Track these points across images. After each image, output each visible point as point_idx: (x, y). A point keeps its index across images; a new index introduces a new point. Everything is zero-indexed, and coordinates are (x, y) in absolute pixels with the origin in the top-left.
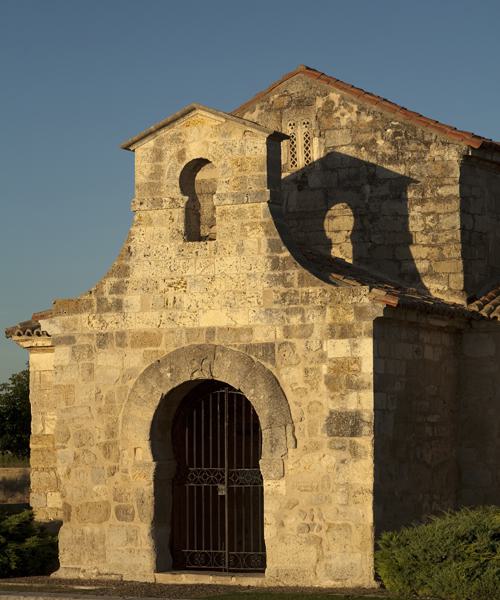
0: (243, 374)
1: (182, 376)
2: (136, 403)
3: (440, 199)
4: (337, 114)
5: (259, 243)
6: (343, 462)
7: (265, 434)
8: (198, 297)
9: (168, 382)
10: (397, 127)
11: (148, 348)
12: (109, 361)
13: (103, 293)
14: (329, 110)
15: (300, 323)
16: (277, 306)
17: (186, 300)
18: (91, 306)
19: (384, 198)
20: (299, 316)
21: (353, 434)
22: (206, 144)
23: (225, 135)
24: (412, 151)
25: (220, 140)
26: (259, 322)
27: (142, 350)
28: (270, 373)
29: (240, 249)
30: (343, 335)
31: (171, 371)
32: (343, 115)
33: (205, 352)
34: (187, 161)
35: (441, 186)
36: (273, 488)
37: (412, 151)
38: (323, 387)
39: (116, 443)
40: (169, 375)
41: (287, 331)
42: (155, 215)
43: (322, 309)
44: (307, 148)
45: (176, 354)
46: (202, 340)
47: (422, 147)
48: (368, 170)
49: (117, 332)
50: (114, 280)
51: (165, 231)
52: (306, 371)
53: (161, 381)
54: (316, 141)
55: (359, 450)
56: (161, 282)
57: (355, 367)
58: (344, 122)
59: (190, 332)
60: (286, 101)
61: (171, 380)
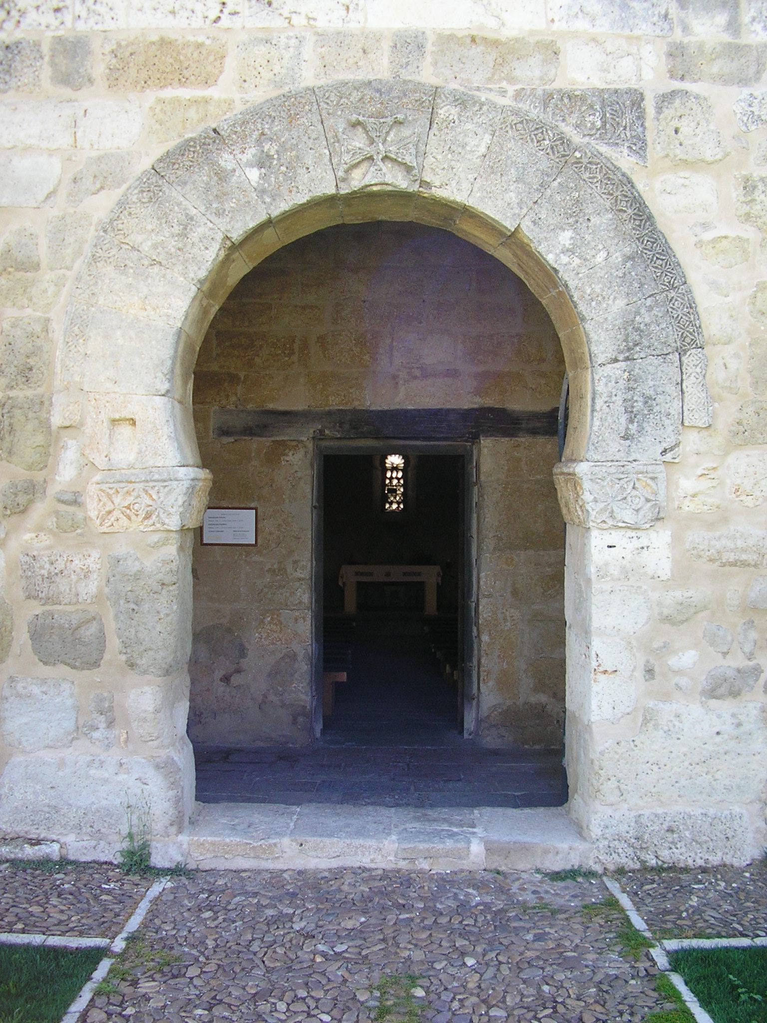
1: (303, 177)
2: (123, 268)
11: (169, 93)
15: (727, 38)
20: (722, 19)
26: (581, 25)
27: (151, 96)
31: (263, 162)
39: (42, 404)
40: (254, 175)
49: (59, 40)
52: (749, 186)
53: (221, 196)
61: (262, 192)
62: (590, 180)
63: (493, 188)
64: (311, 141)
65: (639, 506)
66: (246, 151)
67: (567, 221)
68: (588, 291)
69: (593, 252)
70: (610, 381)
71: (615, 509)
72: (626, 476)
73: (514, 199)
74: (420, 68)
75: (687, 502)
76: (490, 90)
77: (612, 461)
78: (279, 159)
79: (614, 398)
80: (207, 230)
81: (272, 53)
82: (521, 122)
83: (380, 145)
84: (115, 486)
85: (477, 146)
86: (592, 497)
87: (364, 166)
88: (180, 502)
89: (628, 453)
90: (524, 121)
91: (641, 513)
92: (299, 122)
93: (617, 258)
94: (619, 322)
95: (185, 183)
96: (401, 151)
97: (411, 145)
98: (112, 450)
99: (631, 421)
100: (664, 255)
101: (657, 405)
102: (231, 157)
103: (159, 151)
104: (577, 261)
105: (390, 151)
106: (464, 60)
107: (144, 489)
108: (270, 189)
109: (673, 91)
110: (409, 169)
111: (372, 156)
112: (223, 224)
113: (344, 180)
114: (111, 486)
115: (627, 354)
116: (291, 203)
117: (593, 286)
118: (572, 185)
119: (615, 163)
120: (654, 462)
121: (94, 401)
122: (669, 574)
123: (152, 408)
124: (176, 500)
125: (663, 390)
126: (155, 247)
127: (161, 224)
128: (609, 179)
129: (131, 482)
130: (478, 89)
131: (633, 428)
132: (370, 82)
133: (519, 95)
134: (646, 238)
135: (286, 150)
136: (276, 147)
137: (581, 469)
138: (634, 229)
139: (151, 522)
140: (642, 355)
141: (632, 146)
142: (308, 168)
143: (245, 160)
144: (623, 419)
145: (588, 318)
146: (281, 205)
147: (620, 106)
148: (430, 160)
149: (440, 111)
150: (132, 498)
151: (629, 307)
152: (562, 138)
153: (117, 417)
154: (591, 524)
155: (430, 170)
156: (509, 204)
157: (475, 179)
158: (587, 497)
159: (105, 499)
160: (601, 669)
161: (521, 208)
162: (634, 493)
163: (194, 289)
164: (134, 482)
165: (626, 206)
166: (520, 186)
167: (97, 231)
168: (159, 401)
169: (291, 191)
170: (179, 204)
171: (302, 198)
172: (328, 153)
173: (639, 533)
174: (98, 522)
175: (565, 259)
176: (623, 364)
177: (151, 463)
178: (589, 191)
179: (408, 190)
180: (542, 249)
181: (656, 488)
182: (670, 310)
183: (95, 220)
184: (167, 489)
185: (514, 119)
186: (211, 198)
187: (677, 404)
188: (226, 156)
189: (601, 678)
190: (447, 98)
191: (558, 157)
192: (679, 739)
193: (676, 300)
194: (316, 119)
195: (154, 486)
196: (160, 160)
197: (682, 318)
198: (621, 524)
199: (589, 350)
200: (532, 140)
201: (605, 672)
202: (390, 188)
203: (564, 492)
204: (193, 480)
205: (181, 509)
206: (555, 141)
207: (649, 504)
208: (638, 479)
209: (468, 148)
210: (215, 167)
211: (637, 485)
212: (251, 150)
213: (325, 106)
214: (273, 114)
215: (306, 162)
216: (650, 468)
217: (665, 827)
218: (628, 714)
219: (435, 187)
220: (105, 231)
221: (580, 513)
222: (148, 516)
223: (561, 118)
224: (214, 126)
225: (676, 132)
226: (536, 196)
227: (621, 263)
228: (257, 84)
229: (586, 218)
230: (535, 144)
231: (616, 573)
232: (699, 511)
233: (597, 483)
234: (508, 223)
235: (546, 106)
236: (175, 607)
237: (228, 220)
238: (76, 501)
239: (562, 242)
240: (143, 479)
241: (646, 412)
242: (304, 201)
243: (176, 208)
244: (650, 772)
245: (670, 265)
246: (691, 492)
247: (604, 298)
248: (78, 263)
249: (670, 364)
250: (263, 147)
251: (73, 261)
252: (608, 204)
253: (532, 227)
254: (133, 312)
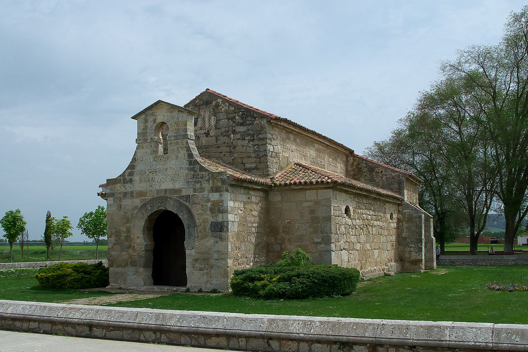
3: (260, 139)
4: (221, 107)
5: (184, 155)
6: (217, 242)
7: (186, 231)
8: (161, 177)
9: (150, 210)
10: (244, 111)
11: (142, 198)
12: (127, 203)
13: (125, 176)
14: (217, 106)
15: (200, 187)
16: (191, 180)
17: (157, 178)
18: (121, 181)
19: (238, 139)
20: (200, 184)
21: (220, 231)
22: (164, 116)
23: (171, 112)
24: (249, 121)
25: (169, 114)
28: (188, 207)
29: (177, 158)
30: (216, 192)
31: (150, 206)
32: (223, 107)
33: (163, 198)
34: (157, 123)
35: (260, 134)
36: (190, 253)
37: (249, 121)
38: (209, 212)
40: (150, 208)
41: (195, 190)
42: (145, 145)
43: (208, 181)
44: (209, 121)
45: (153, 200)
46: (163, 194)
47: (253, 119)
48: (232, 129)
50: (129, 171)
51: (149, 151)
54: (213, 117)
55: (223, 237)
56: (147, 171)
57: (221, 204)
58: (223, 110)
59: (158, 191)
60: (201, 102)
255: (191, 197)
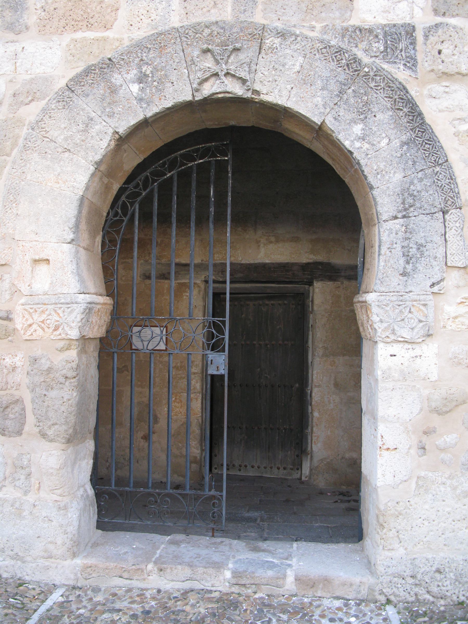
0: (334, 87)
1: (169, 90)
27: (67, 38)
40: (135, 88)
53: (113, 103)
61: (141, 100)
62: (376, 88)
63: (305, 94)
64: (176, 63)
65: (414, 325)
66: (130, 72)
67: (359, 117)
68: (375, 168)
69: (379, 139)
70: (392, 233)
71: (396, 327)
72: (404, 303)
73: (320, 102)
74: (254, 14)
75: (450, 323)
76: (304, 26)
77: (394, 292)
78: (153, 77)
79: (395, 246)
80: (101, 127)
81: (151, 6)
82: (325, 48)
83: (223, 65)
84: (35, 306)
85: (293, 65)
86: (378, 319)
87: (213, 79)
88: (79, 319)
89: (406, 286)
90: (328, 47)
91: (416, 330)
92: (167, 51)
93: (396, 143)
94: (398, 190)
95: (88, 95)
96: (239, 69)
97: (245, 65)
98: (33, 281)
99: (408, 263)
100: (431, 141)
101: (427, 250)
102: (120, 76)
103: (72, 74)
104: (366, 146)
105: (230, 69)
106: (285, 7)
107: (54, 309)
108: (146, 98)
109: (436, 24)
110: (244, 81)
111: (217, 73)
112: (113, 123)
113: (197, 90)
114: (31, 306)
115: (404, 213)
116: (161, 107)
117: (379, 164)
118: (362, 91)
119: (394, 76)
120: (425, 293)
121: (22, 247)
122: (437, 377)
123: (61, 252)
124: (76, 318)
125: (431, 239)
126: (66, 139)
127: (70, 124)
128: (389, 87)
129: (45, 304)
130: (295, 26)
131: (409, 268)
132: (217, 22)
133: (325, 30)
134: (418, 129)
135: (157, 71)
136: (151, 69)
137: (370, 297)
138: (408, 122)
139: (58, 333)
140: (416, 214)
141: (406, 63)
142: (172, 83)
143: (129, 78)
144: (402, 261)
145: (375, 187)
146: (154, 109)
147: (397, 35)
148: (259, 75)
149: (267, 41)
150: (45, 316)
151: (405, 179)
152: (355, 58)
153: (37, 258)
154: (378, 338)
155: (259, 82)
156: (316, 106)
157: (292, 88)
158: (375, 318)
159: (27, 316)
160: (385, 447)
161: (325, 108)
162: (410, 315)
163: (92, 168)
164: (48, 304)
165: (402, 106)
166: (324, 92)
167: (28, 129)
168: (66, 247)
169: (160, 99)
170: (83, 110)
171: (169, 104)
172: (187, 72)
173: (414, 346)
174: (22, 332)
175: (357, 144)
176: (401, 221)
177: (59, 291)
178: (375, 95)
179: (244, 97)
180: (341, 137)
181: (426, 312)
182: (436, 181)
183: (27, 123)
184: (69, 310)
185: (321, 46)
186: (105, 105)
187: (441, 250)
188: (116, 76)
189: (385, 453)
190: (271, 32)
191: (352, 72)
192: (444, 501)
193: (440, 174)
194: (179, 48)
195: (61, 307)
196: (71, 80)
197: (445, 186)
198: (400, 339)
199: (376, 209)
200: (333, 60)
201: (388, 449)
202: (230, 95)
203: (361, 316)
204: (90, 303)
205: (80, 324)
206: (349, 61)
207: (421, 324)
208: (413, 306)
209: (287, 67)
210: (108, 84)
211: (412, 310)
212: (134, 71)
213: (185, 39)
214: (149, 46)
215: (172, 78)
216: (422, 297)
217: (434, 569)
218: (405, 481)
219: (263, 94)
220: (33, 129)
221: (370, 330)
222: (56, 329)
223: (355, 45)
224: (109, 57)
225: (440, 52)
226: (336, 100)
227: (399, 147)
228: (140, 27)
229: (373, 114)
230: (335, 63)
231: (396, 375)
232: (459, 330)
233: (382, 308)
234: (316, 119)
235: (343, 36)
236: (75, 394)
237: (116, 120)
238: (8, 317)
239: (355, 132)
240: (54, 302)
241: (419, 256)
242: (169, 105)
243: (81, 112)
244: (421, 526)
245: (435, 148)
246: (454, 315)
247: (387, 172)
248: (15, 152)
249: (436, 221)
250: (142, 69)
251: (12, 150)
252: (389, 105)
253: (334, 122)
254: (50, 184)
255: (419, 35)
